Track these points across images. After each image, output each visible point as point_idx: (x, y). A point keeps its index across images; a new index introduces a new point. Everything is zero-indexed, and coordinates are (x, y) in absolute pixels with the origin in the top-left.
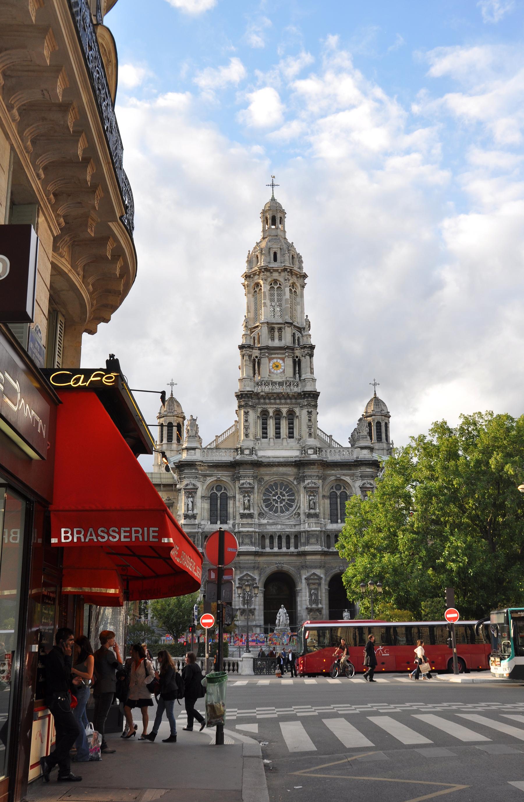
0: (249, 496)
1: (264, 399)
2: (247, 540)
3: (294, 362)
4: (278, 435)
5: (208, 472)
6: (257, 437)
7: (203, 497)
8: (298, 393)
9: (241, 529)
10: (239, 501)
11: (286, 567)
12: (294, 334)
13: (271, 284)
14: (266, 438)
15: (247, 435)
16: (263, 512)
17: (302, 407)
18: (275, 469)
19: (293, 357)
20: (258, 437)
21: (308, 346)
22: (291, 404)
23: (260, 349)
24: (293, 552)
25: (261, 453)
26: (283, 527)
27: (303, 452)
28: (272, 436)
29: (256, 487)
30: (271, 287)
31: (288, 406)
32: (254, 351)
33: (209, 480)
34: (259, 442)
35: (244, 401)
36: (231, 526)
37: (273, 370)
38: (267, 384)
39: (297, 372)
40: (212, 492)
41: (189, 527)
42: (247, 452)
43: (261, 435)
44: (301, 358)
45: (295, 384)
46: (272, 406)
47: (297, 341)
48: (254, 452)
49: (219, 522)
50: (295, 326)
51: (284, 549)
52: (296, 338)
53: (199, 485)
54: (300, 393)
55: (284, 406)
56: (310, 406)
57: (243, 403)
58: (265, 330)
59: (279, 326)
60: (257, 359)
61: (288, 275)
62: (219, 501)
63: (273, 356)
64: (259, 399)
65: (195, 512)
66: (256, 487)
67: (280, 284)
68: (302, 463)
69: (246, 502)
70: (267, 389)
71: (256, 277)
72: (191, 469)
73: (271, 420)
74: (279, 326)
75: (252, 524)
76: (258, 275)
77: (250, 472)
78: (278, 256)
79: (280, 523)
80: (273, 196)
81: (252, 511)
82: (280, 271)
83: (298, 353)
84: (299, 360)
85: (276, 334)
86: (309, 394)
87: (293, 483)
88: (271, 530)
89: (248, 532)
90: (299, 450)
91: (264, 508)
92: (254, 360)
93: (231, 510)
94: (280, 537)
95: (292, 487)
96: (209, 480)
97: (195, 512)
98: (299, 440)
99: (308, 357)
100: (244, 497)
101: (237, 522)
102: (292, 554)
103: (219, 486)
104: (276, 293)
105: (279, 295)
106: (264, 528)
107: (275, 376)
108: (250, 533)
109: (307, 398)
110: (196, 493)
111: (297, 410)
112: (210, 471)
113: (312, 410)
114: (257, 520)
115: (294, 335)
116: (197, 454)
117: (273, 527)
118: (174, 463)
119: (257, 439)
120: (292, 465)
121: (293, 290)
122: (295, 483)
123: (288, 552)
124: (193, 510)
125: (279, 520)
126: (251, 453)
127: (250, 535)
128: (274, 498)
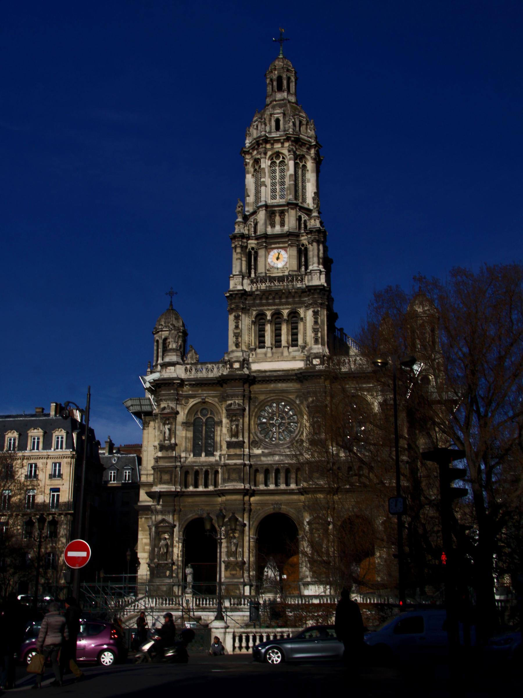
0: (238, 420)
1: (261, 299)
2: (234, 476)
3: (300, 252)
4: (277, 343)
5: (190, 392)
6: (251, 347)
7: (183, 423)
8: (302, 289)
9: (227, 462)
10: (226, 427)
11: (284, 509)
12: (300, 217)
13: (272, 159)
14: (263, 347)
15: (237, 345)
16: (257, 439)
17: (307, 307)
18: (272, 386)
19: (298, 246)
20: (253, 346)
22: (294, 303)
24: (293, 490)
25: (255, 367)
26: (282, 458)
27: (308, 362)
28: (269, 345)
29: (247, 408)
30: (271, 164)
31: (290, 307)
32: (250, 242)
33: (192, 402)
34: (254, 353)
35: (235, 303)
36: (217, 458)
38: (263, 280)
39: (303, 263)
40: (196, 416)
41: (166, 460)
42: (237, 365)
43: (257, 344)
44: (308, 247)
45: (299, 278)
46: (270, 308)
47: (303, 226)
48: (246, 365)
49: (203, 454)
50: (302, 209)
51: (283, 487)
52: (303, 222)
53: (179, 409)
54: (305, 289)
55: (285, 307)
56: (316, 304)
57: (233, 306)
58: (262, 215)
60: (253, 252)
61: (292, 145)
62: (204, 428)
63: (273, 246)
64: (254, 299)
65: (173, 441)
66: (247, 408)
67: (283, 158)
68: (304, 376)
69: (234, 427)
70: (263, 286)
72: (170, 390)
73: (269, 325)
75: (240, 455)
77: (239, 390)
78: (281, 122)
79: (278, 453)
81: (241, 439)
82: (282, 141)
83: (304, 239)
84: (306, 249)
85: (278, 219)
86: (315, 290)
87: (295, 403)
88: (267, 462)
89: (235, 464)
90: (303, 360)
91: (259, 434)
92: (250, 252)
93: (218, 439)
94: (277, 471)
95: (294, 408)
96: (192, 402)
97: (173, 441)
98: (304, 348)
99: (315, 244)
100: (231, 421)
101: (224, 452)
102: (291, 492)
103: (203, 407)
104: (277, 168)
105: (282, 171)
106: (258, 459)
107: (276, 271)
108: (238, 467)
109: (313, 294)
110: (175, 418)
111: (301, 311)
112: (192, 391)
113: (319, 309)
114: (247, 450)
115: (299, 219)
116: (178, 371)
117: (269, 458)
118: (150, 383)
119: (251, 350)
120: (293, 379)
121: (301, 164)
122: (298, 402)
123: (287, 490)
124: (170, 439)
125: (277, 450)
126: (242, 367)
127: (238, 468)
128: (271, 422)
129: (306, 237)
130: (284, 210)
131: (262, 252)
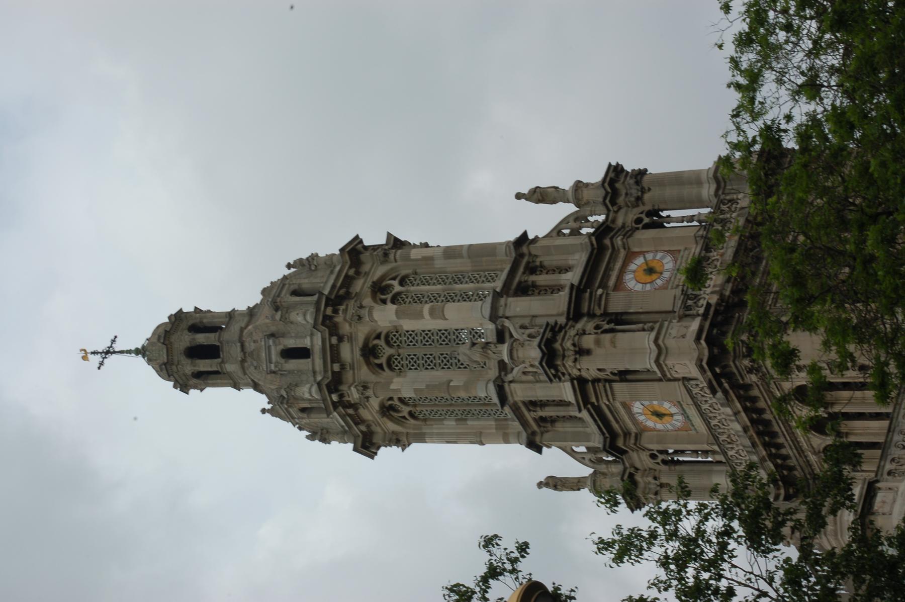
21: (611, 175)
23: (575, 314)
30: (393, 302)
37: (659, 282)
44: (648, 207)
59: (521, 270)
63: (612, 282)
67: (394, 279)
71: (347, 352)
74: (521, 270)
76: (341, 339)
80: (137, 352)
129: (622, 212)
130: (528, 263)
131: (617, 304)
